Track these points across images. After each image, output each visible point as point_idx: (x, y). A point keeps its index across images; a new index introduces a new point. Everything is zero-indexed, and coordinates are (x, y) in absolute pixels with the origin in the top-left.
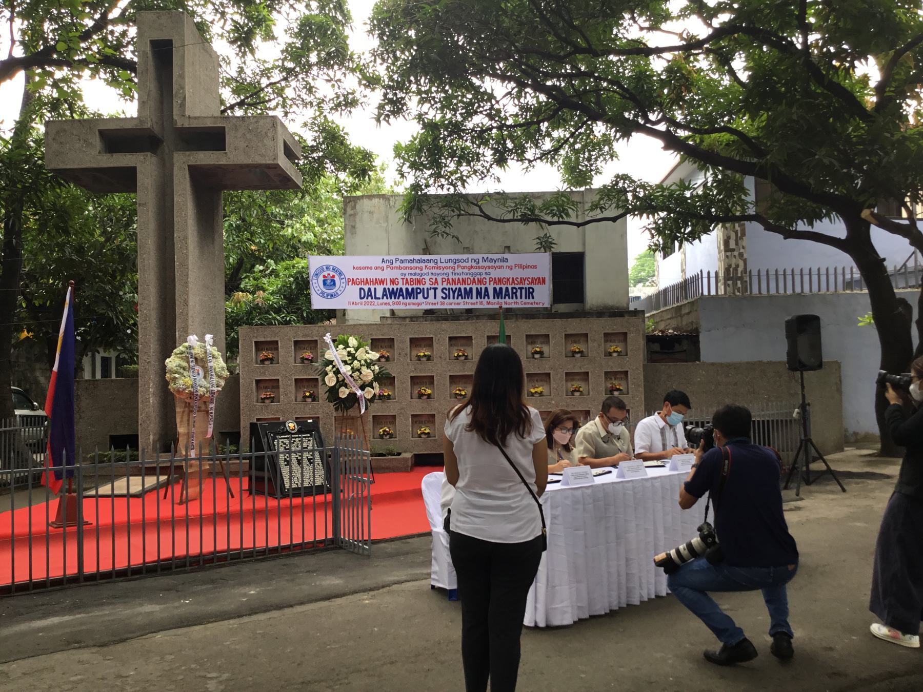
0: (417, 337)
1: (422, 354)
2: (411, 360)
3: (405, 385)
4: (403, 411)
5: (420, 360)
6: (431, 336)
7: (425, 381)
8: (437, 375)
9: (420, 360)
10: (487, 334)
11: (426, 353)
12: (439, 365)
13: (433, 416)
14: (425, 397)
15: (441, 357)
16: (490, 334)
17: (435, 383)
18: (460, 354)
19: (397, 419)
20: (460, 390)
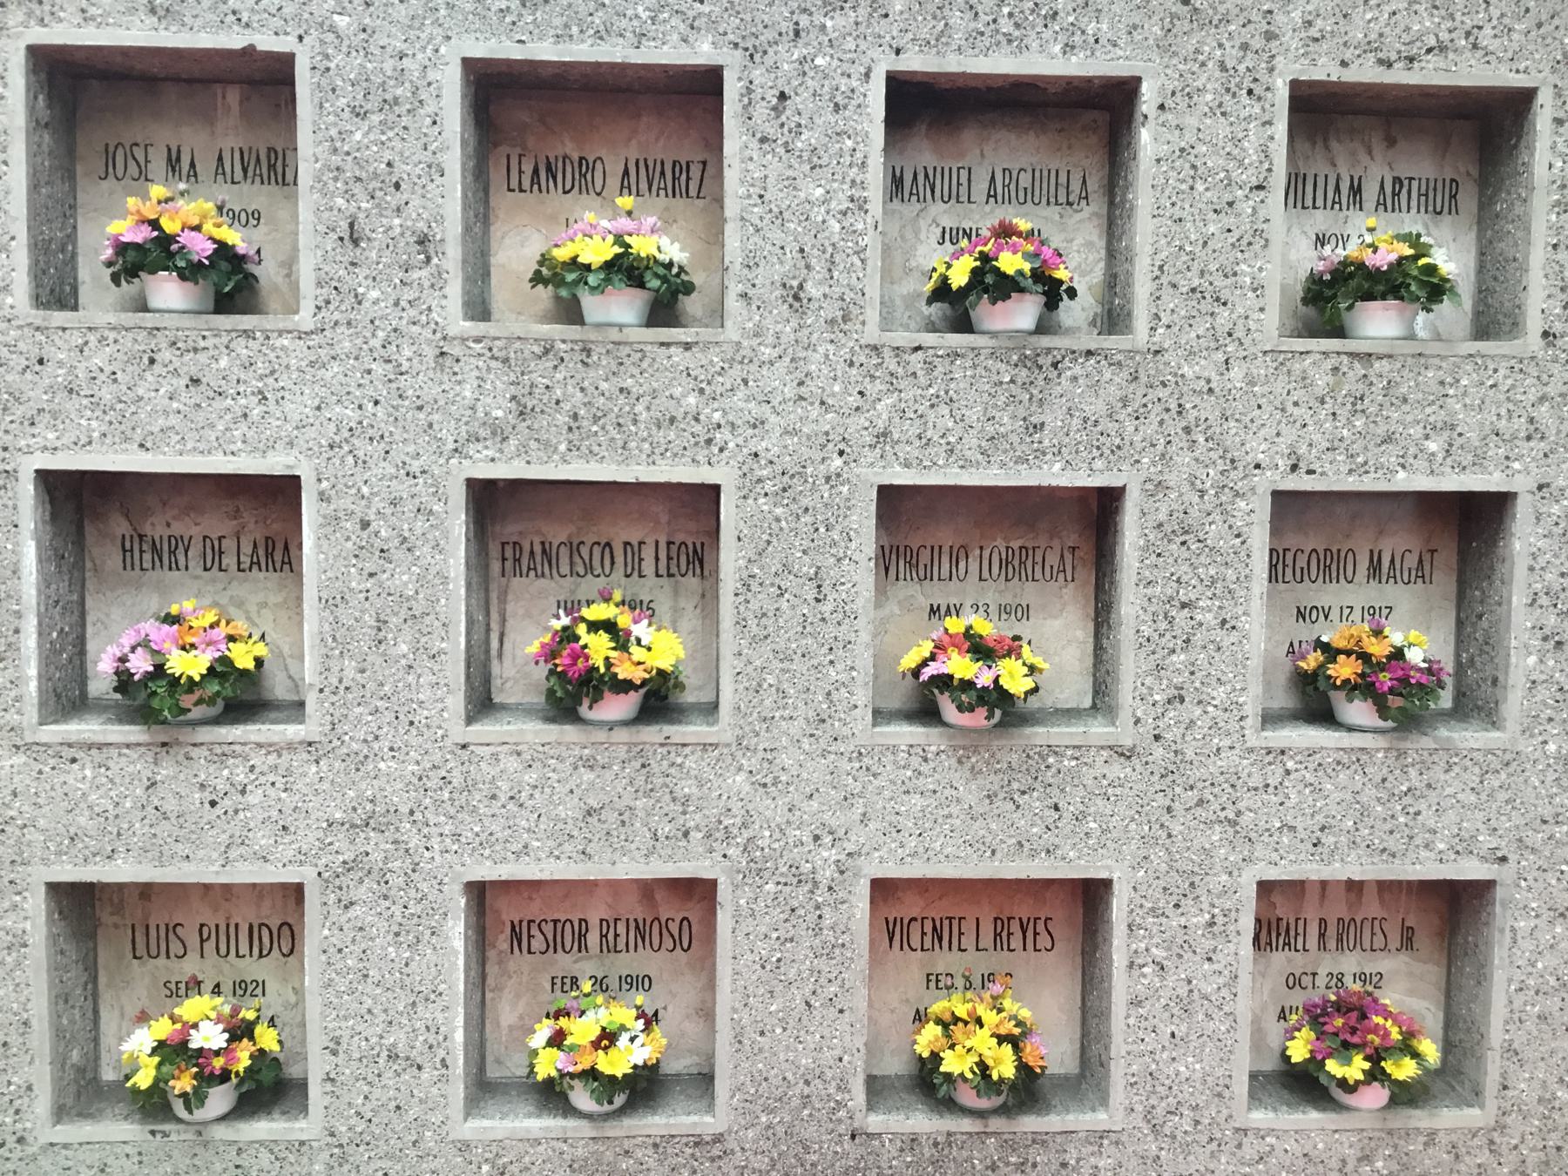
0: (545, 51)
1: (597, 252)
2: (479, 309)
3: (402, 579)
4: (376, 846)
5: (571, 313)
6: (703, 52)
7: (622, 533)
8: (751, 486)
9: (571, 313)
10: (1291, 67)
11: (643, 246)
12: (779, 381)
13: (700, 892)
14: (617, 707)
15: (796, 297)
16: (1325, 70)
17: (730, 559)
18: (1010, 263)
19: (316, 931)
20: (981, 650)
